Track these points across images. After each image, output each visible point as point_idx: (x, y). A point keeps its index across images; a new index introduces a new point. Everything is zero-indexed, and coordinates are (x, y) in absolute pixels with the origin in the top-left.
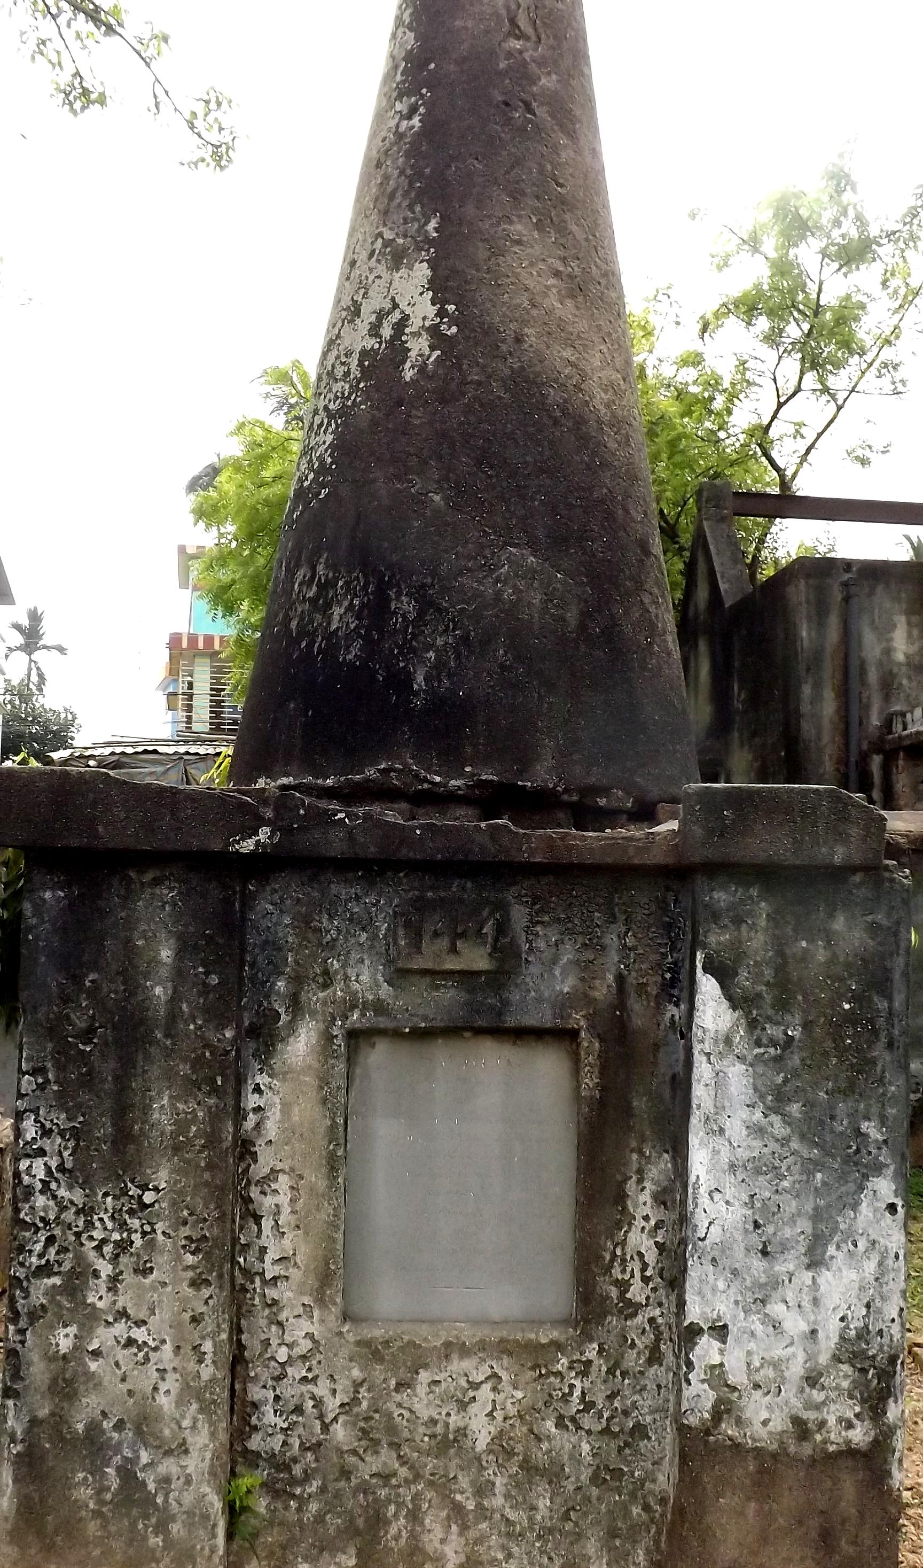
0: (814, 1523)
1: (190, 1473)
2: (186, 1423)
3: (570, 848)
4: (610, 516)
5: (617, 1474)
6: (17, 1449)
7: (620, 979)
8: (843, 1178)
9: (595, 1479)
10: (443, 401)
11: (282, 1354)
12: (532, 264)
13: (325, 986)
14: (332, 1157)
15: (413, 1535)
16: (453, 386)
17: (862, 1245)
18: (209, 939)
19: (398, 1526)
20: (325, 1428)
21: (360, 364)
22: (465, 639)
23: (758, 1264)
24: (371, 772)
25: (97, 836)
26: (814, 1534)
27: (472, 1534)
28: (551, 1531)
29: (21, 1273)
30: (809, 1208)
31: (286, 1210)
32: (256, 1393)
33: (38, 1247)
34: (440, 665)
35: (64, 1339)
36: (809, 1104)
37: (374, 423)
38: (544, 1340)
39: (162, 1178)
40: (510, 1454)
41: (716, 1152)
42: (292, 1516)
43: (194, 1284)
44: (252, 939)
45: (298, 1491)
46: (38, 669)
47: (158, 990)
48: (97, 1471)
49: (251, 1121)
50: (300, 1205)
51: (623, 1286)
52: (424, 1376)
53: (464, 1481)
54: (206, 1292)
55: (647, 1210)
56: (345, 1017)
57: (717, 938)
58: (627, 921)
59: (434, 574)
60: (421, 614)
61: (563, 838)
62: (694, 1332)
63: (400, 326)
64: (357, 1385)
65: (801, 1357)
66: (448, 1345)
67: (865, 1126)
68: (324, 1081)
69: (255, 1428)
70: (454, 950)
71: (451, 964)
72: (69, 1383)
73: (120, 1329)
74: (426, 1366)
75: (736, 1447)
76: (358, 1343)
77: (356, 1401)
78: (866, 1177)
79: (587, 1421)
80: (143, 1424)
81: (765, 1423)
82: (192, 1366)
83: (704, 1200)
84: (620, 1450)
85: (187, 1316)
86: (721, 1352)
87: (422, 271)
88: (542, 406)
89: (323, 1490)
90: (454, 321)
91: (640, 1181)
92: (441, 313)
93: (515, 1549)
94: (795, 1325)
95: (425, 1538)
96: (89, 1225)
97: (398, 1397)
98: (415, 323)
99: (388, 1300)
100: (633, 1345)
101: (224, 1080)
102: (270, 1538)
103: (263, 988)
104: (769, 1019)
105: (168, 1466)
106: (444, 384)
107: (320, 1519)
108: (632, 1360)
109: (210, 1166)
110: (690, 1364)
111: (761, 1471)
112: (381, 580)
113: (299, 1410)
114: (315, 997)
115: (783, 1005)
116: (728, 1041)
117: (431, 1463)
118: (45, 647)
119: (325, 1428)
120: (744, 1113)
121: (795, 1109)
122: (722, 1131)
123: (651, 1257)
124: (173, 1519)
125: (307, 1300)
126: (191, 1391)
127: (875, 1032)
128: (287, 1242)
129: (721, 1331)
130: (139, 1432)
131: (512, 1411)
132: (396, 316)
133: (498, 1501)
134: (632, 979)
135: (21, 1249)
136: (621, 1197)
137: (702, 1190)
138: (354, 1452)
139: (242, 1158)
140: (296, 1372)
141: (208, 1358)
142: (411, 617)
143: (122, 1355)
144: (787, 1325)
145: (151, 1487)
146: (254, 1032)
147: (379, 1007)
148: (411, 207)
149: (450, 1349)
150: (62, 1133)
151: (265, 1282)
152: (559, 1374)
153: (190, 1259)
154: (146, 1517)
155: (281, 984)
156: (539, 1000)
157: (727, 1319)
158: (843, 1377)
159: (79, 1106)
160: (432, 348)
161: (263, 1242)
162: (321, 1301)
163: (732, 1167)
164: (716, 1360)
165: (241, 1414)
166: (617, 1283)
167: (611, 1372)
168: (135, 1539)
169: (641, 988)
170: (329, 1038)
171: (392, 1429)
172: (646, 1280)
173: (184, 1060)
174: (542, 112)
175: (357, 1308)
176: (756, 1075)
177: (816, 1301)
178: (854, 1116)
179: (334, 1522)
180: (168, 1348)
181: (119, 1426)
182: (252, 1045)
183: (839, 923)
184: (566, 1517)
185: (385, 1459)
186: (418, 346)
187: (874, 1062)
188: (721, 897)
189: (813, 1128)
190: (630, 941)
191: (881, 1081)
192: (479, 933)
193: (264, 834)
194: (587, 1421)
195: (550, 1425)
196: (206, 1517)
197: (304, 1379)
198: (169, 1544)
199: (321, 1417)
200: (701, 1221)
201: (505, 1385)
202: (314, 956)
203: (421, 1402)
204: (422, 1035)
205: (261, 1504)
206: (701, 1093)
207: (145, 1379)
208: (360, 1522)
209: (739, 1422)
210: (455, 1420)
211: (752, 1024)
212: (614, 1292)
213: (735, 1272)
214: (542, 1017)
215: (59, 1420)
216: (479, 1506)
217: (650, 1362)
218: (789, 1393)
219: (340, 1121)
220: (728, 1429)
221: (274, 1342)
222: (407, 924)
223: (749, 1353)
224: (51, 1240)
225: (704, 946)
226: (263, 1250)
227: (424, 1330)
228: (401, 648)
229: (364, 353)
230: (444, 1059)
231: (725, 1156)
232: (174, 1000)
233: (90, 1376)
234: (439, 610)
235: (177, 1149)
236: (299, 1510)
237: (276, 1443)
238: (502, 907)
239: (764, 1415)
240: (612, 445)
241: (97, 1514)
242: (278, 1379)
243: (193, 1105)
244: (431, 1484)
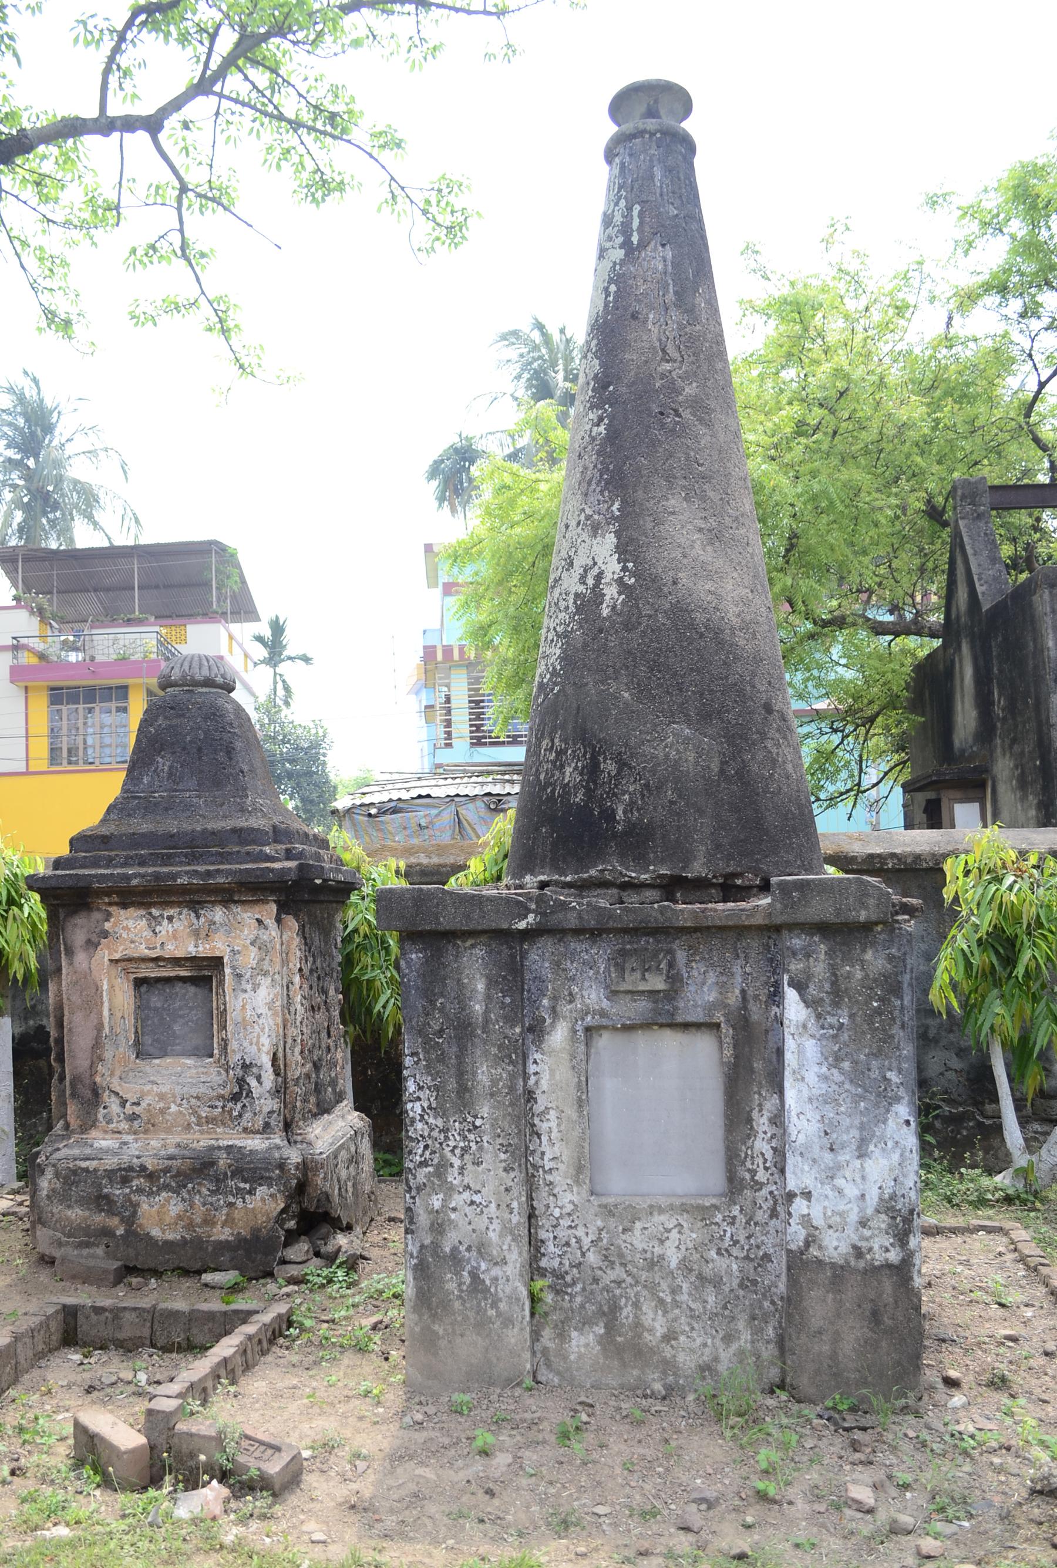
0: (868, 1306)
1: (509, 1276)
2: (505, 1247)
3: (706, 917)
4: (741, 693)
5: (754, 1283)
6: (414, 1261)
7: (743, 992)
8: (877, 1105)
9: (741, 1285)
10: (629, 631)
11: (557, 1212)
12: (683, 527)
13: (571, 1002)
14: (580, 1100)
15: (636, 1317)
16: (634, 619)
17: (890, 1144)
18: (504, 978)
19: (627, 1312)
20: (583, 1254)
21: (575, 603)
22: (647, 786)
23: (828, 1156)
24: (593, 872)
25: (440, 923)
26: (867, 1313)
27: (670, 1316)
28: (716, 1315)
29: (411, 1165)
30: (857, 1122)
31: (555, 1130)
32: (543, 1235)
33: (420, 1151)
34: (632, 803)
35: (436, 1202)
36: (855, 1062)
37: (585, 645)
38: (707, 1204)
39: (485, 1111)
40: (691, 1270)
41: (800, 1091)
42: (566, 1305)
43: (505, 1170)
44: (528, 976)
45: (569, 1290)
46: (284, 681)
47: (477, 1007)
48: (458, 1273)
49: (532, 1080)
50: (563, 1127)
51: (753, 1172)
52: (638, 1225)
53: (664, 1285)
54: (512, 1175)
55: (765, 1128)
56: (583, 1019)
57: (796, 966)
58: (746, 958)
59: (626, 745)
60: (619, 773)
61: (704, 911)
62: (791, 1196)
63: (599, 577)
64: (600, 1230)
65: (856, 1210)
66: (651, 1206)
67: (889, 1074)
68: (573, 1057)
69: (543, 1255)
70: (644, 979)
71: (642, 987)
72: (440, 1225)
73: (466, 1195)
74: (639, 1219)
75: (820, 1262)
76: (600, 1206)
77: (600, 1239)
78: (890, 1104)
79: (735, 1251)
80: (481, 1248)
81: (836, 1248)
82: (507, 1216)
83: (794, 1119)
84: (755, 1268)
85: (502, 1188)
86: (808, 1207)
87: (611, 539)
88: (692, 626)
89: (584, 1289)
90: (633, 574)
91: (760, 1111)
92: (624, 569)
93: (696, 1325)
94: (852, 1191)
95: (643, 1317)
96: (447, 1138)
97: (624, 1237)
98: (608, 577)
99: (617, 1183)
100: (761, 1207)
101: (516, 1056)
102: (554, 1317)
103: (535, 1004)
104: (829, 1013)
105: (496, 1271)
106: (628, 619)
107: (582, 1306)
108: (761, 1216)
109: (512, 1104)
110: (790, 1214)
111: (834, 1276)
112: (594, 750)
113: (567, 1244)
114: (565, 1008)
115: (836, 1004)
116: (804, 1026)
117: (644, 1275)
118: (290, 658)
119: (583, 1254)
120: (816, 1068)
121: (846, 1065)
122: (803, 1079)
123: (769, 1155)
124: (500, 1300)
125: (569, 1181)
126: (507, 1229)
127: (893, 1019)
128: (556, 1148)
129: (807, 1195)
130: (479, 1251)
131: (691, 1245)
132: (595, 571)
133: (685, 1297)
134: (750, 992)
135: (410, 1152)
136: (749, 1120)
137: (793, 1114)
138: (600, 1268)
139: (528, 1101)
140: (565, 1222)
141: (516, 1211)
142: (613, 773)
143: (468, 1210)
144: (846, 1191)
145: (488, 1282)
146: (531, 1029)
147: (603, 1014)
148: (602, 492)
149: (652, 1210)
150: (429, 1088)
151: (545, 1172)
152: (717, 1224)
153: (503, 1156)
154: (486, 1299)
155: (545, 1002)
156: (695, 1006)
157: (811, 1188)
158: (882, 1221)
159: (437, 1073)
160: (620, 593)
161: (543, 1149)
162: (577, 1182)
163: (810, 1100)
164: (805, 1211)
165: (535, 1246)
166: (749, 1170)
167: (748, 1223)
168: (479, 1311)
169: (756, 997)
170: (575, 1032)
171: (621, 1255)
172: (766, 1169)
173: (493, 1045)
174: (686, 414)
175: (598, 1188)
176: (822, 1046)
177: (863, 1178)
178: (881, 1068)
179: (591, 1308)
180: (493, 1206)
181: (469, 1249)
182: (531, 1036)
183: (869, 956)
184: (725, 1307)
185: (618, 1273)
186: (611, 592)
187: (892, 1037)
188: (797, 942)
189: (858, 1076)
190: (748, 969)
191: (898, 1048)
192: (658, 968)
193: (531, 918)
194: (735, 1251)
195: (713, 1253)
196: (518, 1300)
197: (570, 1227)
198: (499, 1314)
199: (580, 1248)
200: (792, 1131)
201: (686, 1230)
202: (563, 984)
203: (638, 1239)
204: (628, 1028)
205: (549, 1298)
206: (790, 1058)
207: (481, 1223)
208: (605, 1308)
209: (820, 1247)
210: (657, 1250)
211: (819, 1016)
212: (748, 1176)
213: (814, 1161)
215: (436, 1246)
216: (674, 1300)
217: (771, 1217)
218: (850, 1231)
219: (583, 1079)
220: (814, 1251)
221: (552, 1205)
222: (616, 965)
223: (825, 1208)
224: (426, 1147)
225: (788, 971)
226: (543, 1153)
227: (638, 1199)
228: (608, 793)
229: (577, 595)
230: (642, 1041)
231: (806, 1093)
232: (487, 1011)
233: (451, 1222)
234: (630, 768)
235: (492, 1095)
236: (570, 1301)
237: (555, 1263)
238: (670, 952)
239: (835, 1243)
240: (742, 643)
241: (460, 1297)
242: (555, 1226)
243: (500, 1070)
244: (645, 1286)
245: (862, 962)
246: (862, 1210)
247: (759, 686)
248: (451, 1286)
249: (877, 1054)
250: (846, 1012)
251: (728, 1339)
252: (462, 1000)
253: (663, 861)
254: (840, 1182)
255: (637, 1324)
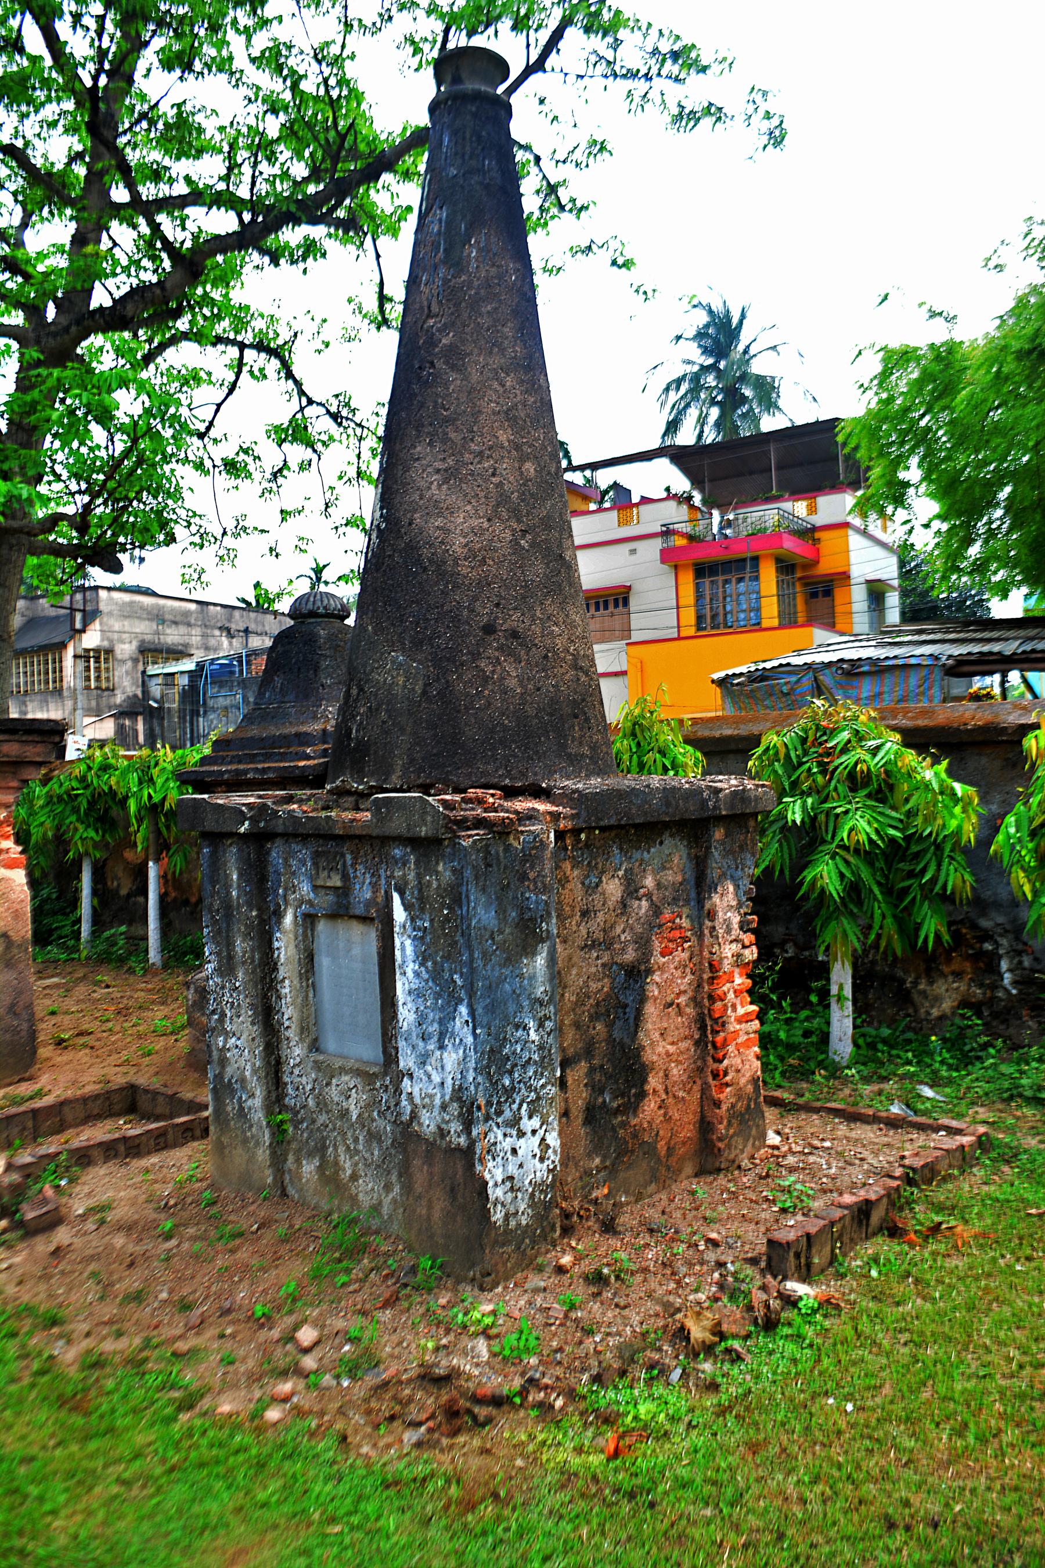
0: (448, 1182)
4: (456, 620)
23: (421, 1044)
36: (435, 963)
44: (271, 869)
80: (243, 1080)
88: (418, 562)
94: (436, 1078)
99: (331, 1044)
102: (294, 1146)
126: (255, 1071)
147: (310, 902)
149: (342, 1070)
158: (454, 1108)
183: (440, 868)
185: (322, 1118)
188: (397, 852)
189: (436, 975)
200: (401, 1018)
207: (242, 1062)
209: (420, 1124)
211: (413, 920)
214: (359, 910)
238: (343, 856)
245: (437, 873)
246: (443, 1096)
247: (478, 609)
248: (229, 1108)
249: (447, 957)
250: (427, 917)
251: (388, 1188)
252: (227, 887)
253: (372, 774)
254: (429, 1068)
255: (336, 1163)
